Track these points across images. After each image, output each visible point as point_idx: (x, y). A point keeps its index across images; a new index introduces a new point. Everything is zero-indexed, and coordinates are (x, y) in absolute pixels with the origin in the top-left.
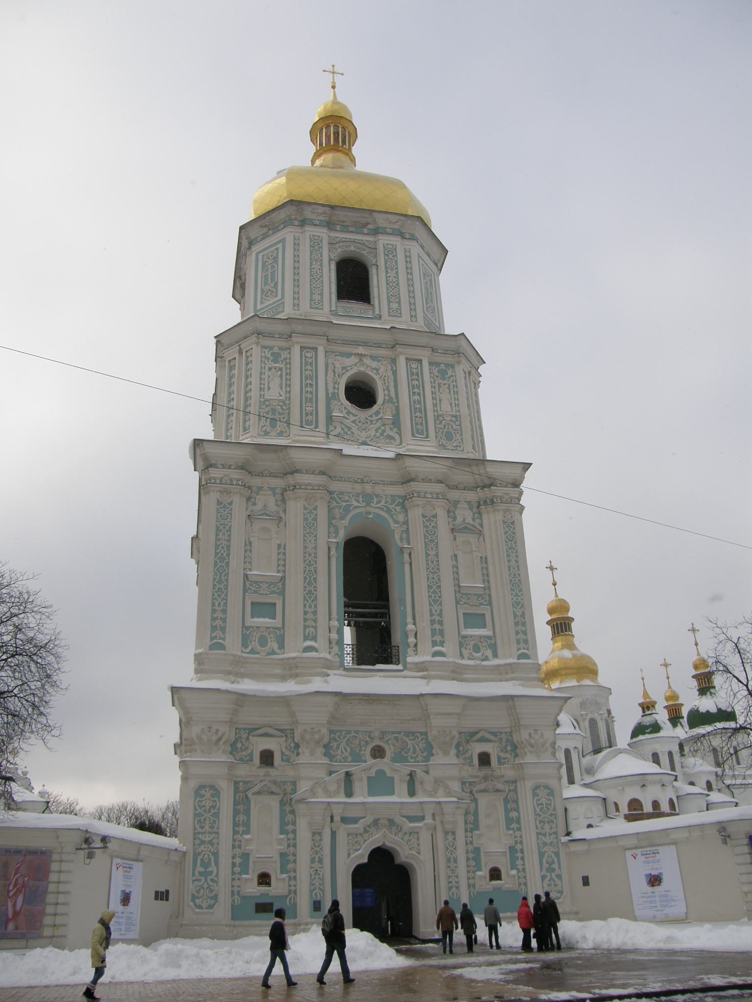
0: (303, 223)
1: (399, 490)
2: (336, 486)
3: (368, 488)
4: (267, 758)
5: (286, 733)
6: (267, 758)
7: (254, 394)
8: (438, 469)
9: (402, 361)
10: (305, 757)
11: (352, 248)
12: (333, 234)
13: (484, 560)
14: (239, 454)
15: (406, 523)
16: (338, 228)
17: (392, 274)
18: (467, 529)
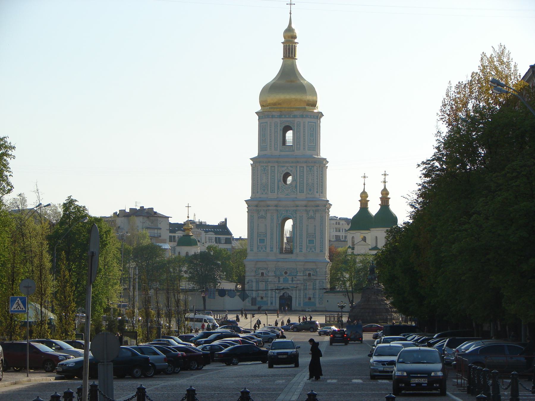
0: (273, 117)
1: (295, 208)
2: (279, 208)
3: (287, 208)
4: (262, 274)
5: (266, 269)
6: (262, 274)
7: (259, 181)
8: (304, 203)
9: (298, 167)
10: (270, 274)
11: (287, 124)
12: (281, 119)
13: (315, 226)
14: (256, 203)
15: (296, 217)
16: (283, 116)
17: (298, 134)
18: (312, 218)
